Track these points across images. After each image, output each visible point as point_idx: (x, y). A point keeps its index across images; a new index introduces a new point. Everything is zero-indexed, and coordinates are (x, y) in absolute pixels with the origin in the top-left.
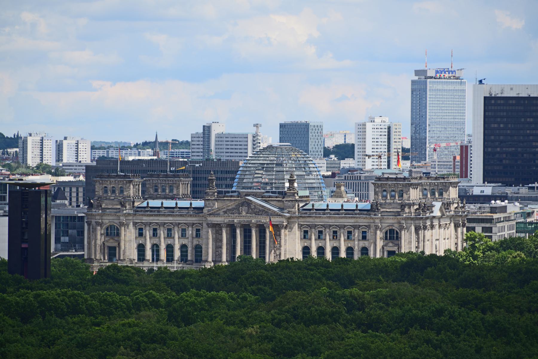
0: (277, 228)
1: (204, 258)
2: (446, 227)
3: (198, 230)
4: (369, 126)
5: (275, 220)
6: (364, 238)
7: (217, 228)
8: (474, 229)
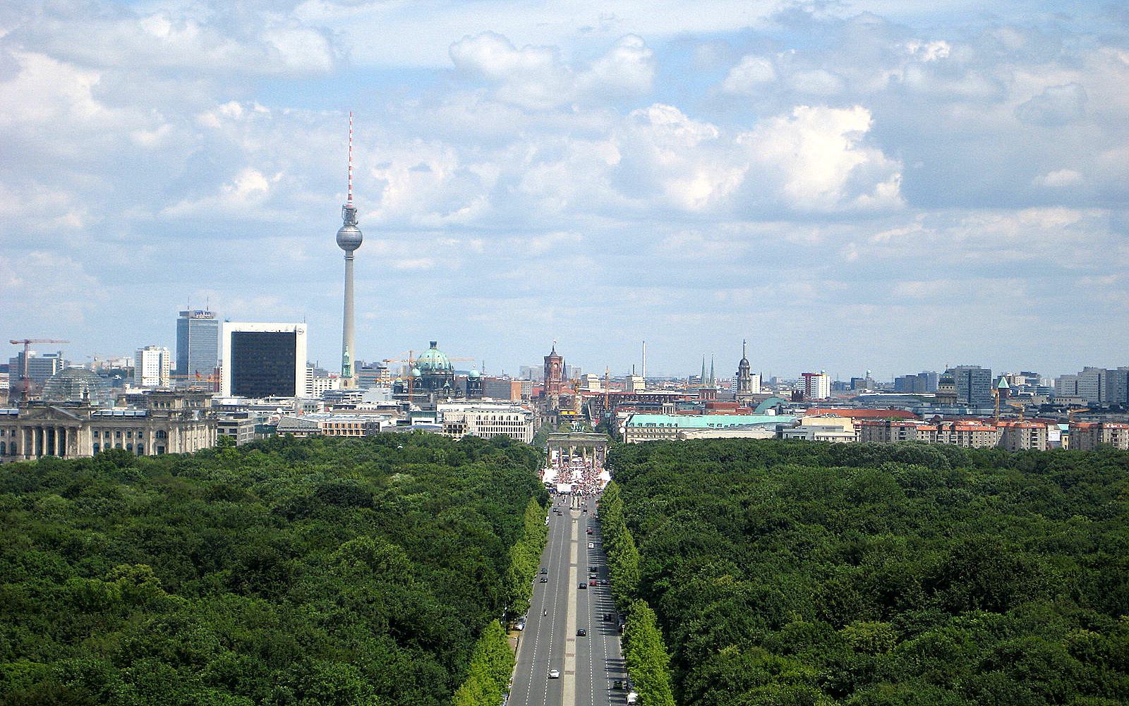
0: (74, 430)
1: (17, 452)
2: (203, 429)
3: (13, 431)
4: (145, 353)
5: (72, 424)
6: (140, 437)
7: (28, 430)
8: (223, 431)
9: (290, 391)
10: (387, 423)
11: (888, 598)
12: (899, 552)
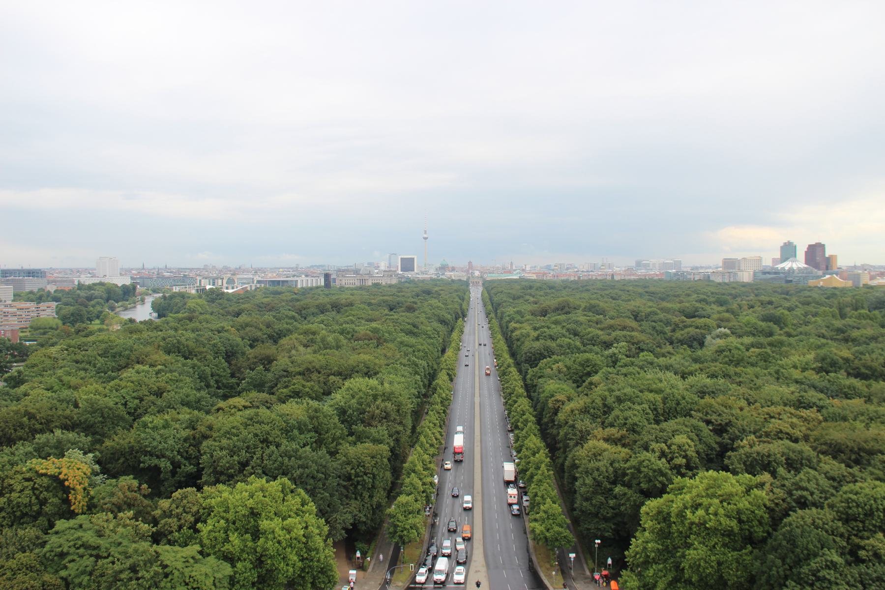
9: (413, 270)
10: (434, 277)
11: (544, 313)
12: (551, 302)
